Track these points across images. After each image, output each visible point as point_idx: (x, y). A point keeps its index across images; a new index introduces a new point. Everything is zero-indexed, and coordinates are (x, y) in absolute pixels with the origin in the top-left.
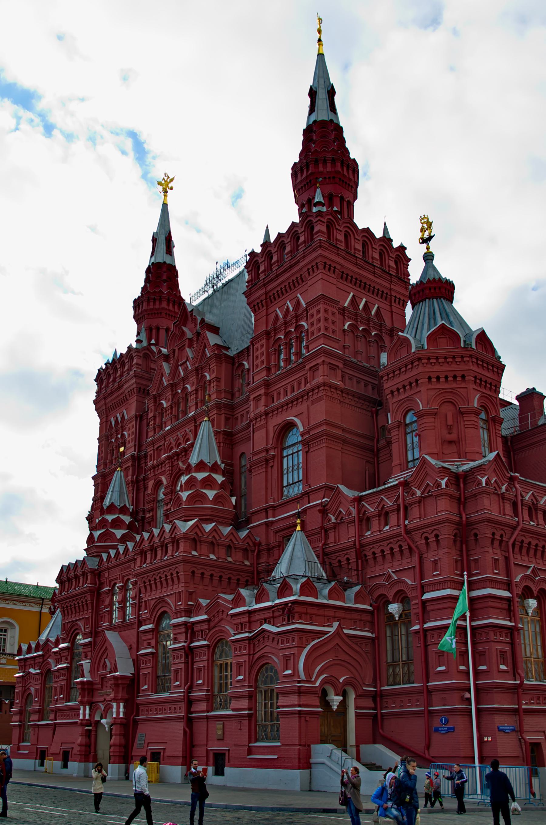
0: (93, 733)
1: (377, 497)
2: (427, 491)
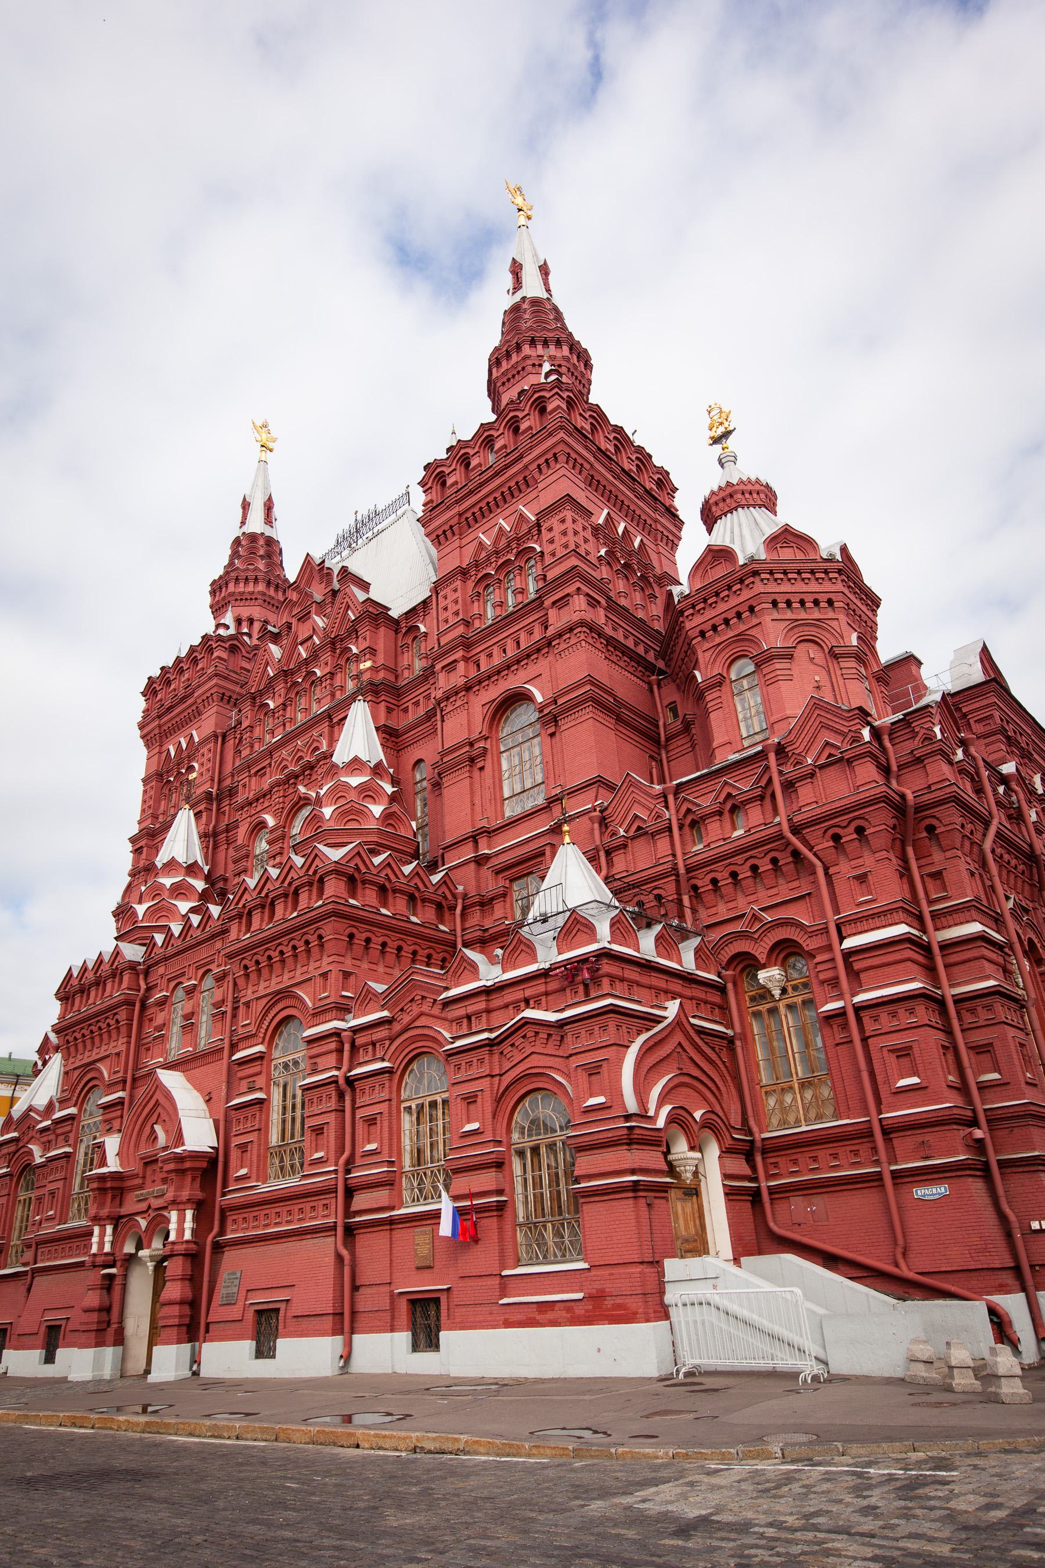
0: (118, 1281)
1: (717, 781)
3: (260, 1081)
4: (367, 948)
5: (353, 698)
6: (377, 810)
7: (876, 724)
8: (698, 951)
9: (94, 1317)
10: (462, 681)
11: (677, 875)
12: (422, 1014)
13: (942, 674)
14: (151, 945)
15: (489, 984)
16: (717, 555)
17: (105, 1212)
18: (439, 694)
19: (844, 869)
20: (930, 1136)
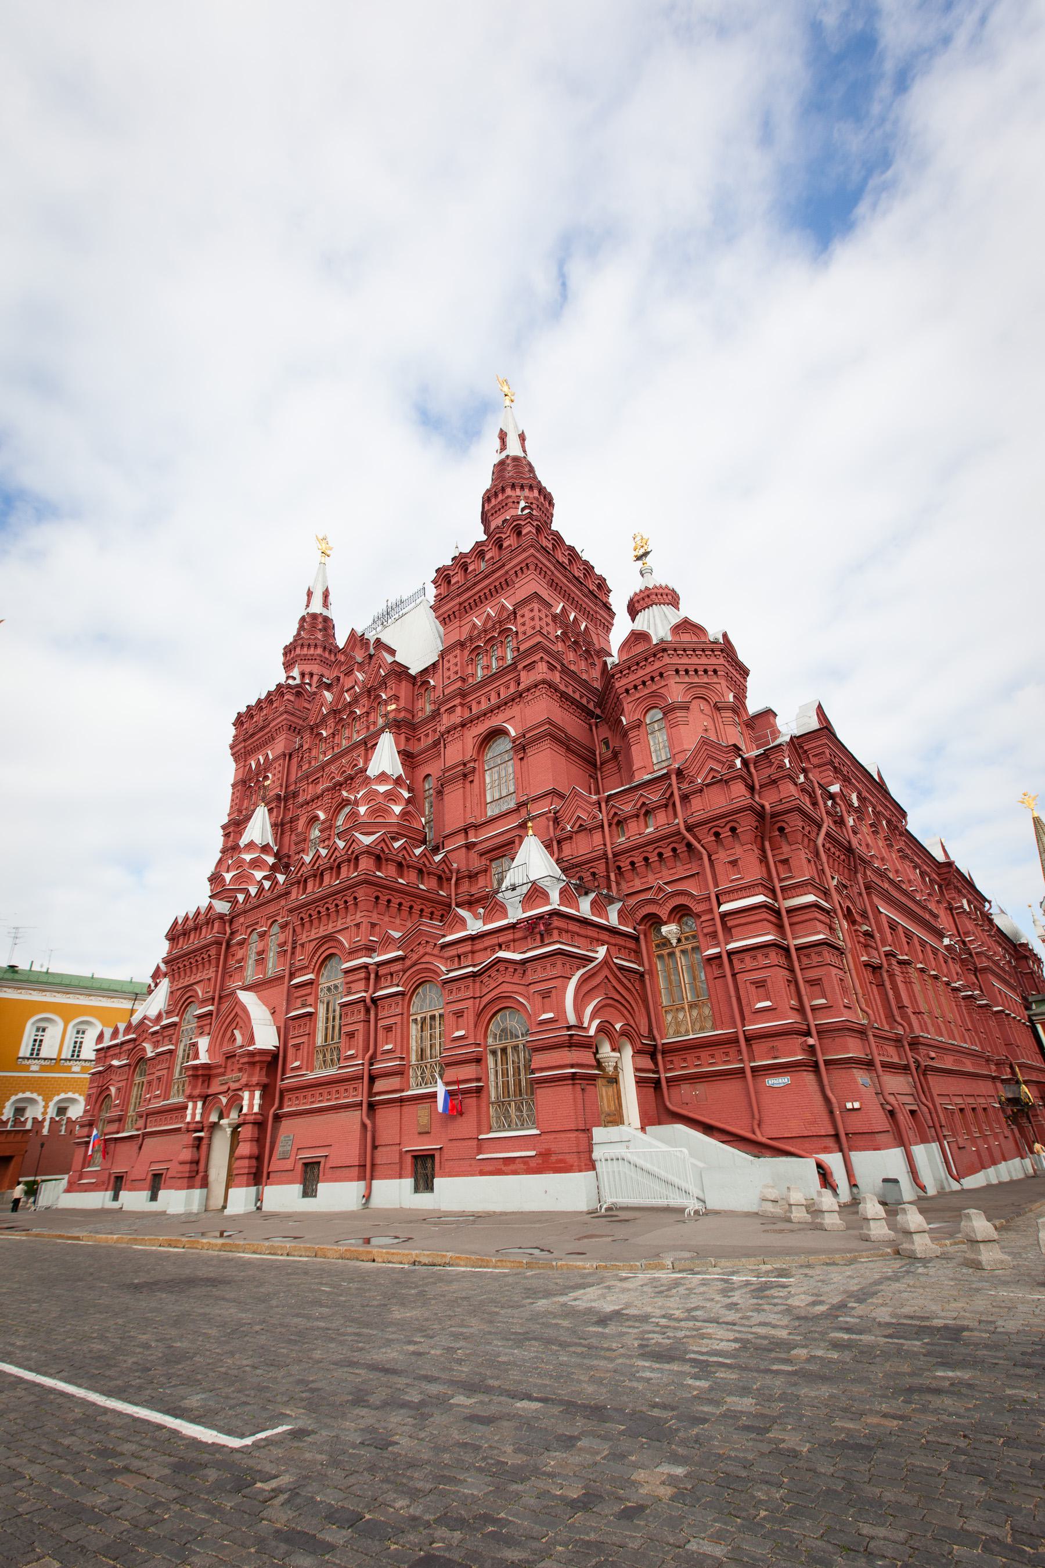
0: (205, 1142)
2: (710, 776)
3: (311, 1000)
4: (388, 906)
5: (382, 730)
6: (397, 809)
7: (745, 756)
8: (620, 912)
9: (187, 1167)
10: (459, 720)
11: (607, 859)
12: (426, 954)
13: (791, 723)
14: (235, 902)
15: (474, 933)
16: (638, 637)
17: (197, 1092)
18: (443, 729)
19: (722, 856)
20: (778, 1043)
